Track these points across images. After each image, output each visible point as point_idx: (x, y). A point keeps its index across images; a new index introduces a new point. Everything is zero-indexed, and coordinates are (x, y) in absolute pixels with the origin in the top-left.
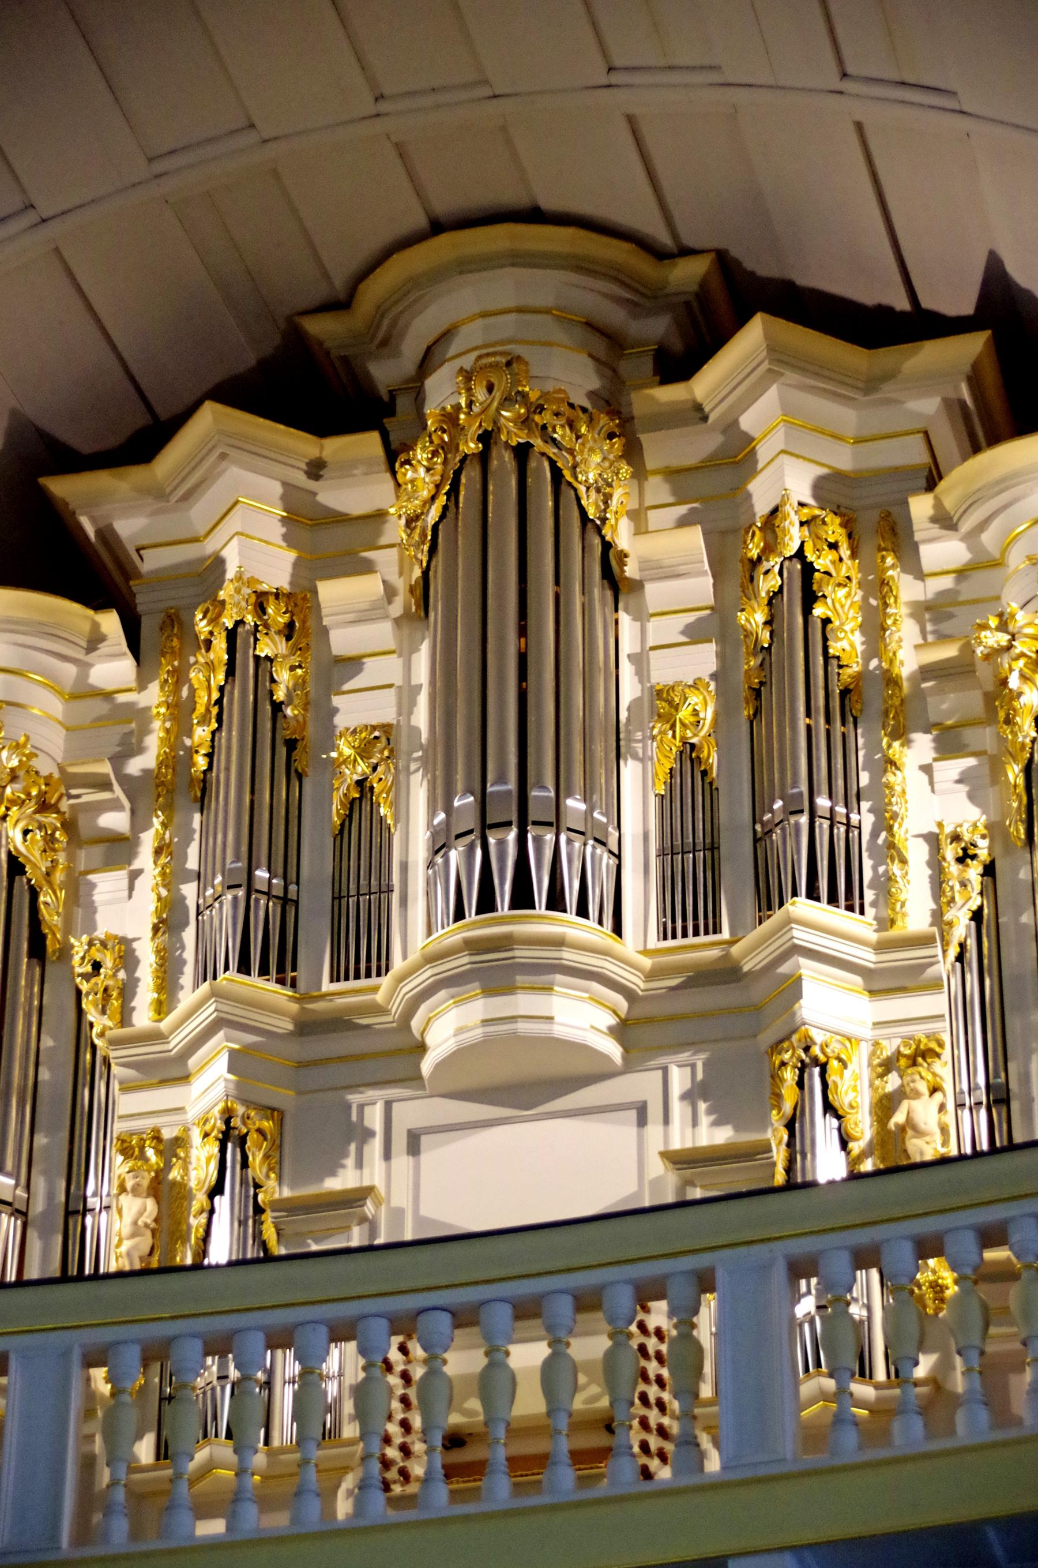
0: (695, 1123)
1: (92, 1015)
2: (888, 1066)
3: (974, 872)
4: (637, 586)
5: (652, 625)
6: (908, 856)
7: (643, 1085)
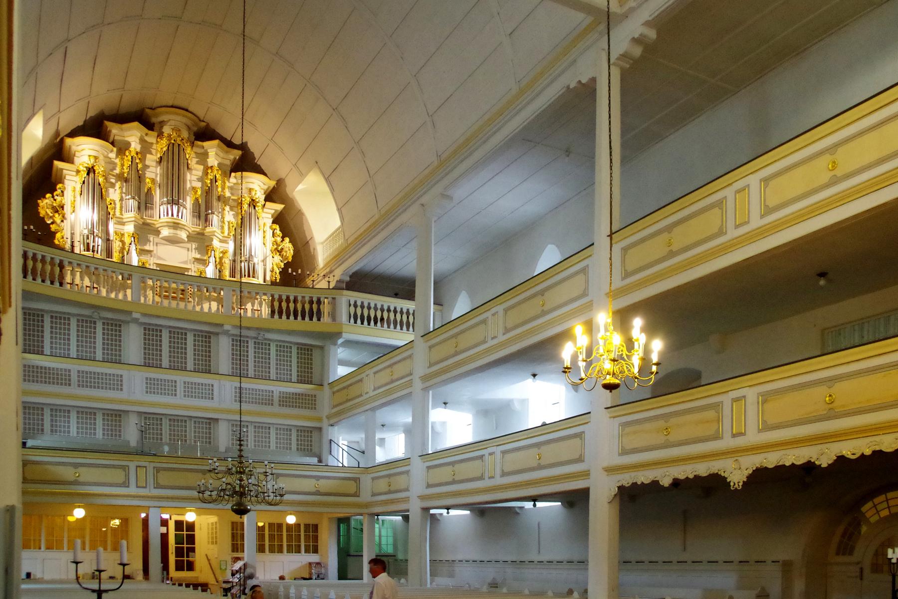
7: (189, 245)
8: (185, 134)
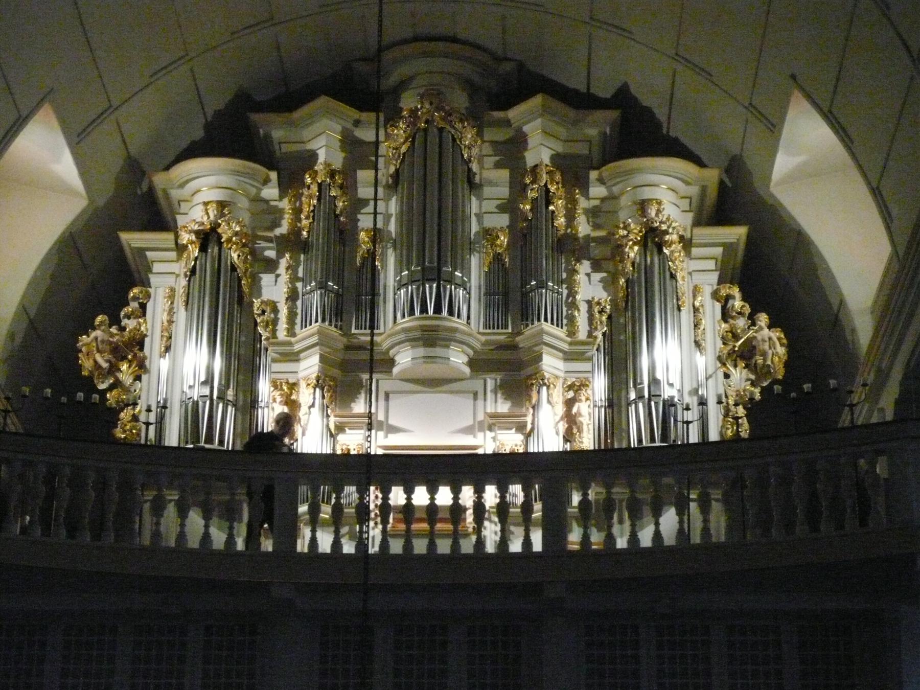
0: (496, 401)
1: (260, 330)
2: (570, 387)
3: (604, 318)
4: (480, 186)
5: (485, 203)
6: (581, 309)
7: (477, 384)
8: (460, 100)
